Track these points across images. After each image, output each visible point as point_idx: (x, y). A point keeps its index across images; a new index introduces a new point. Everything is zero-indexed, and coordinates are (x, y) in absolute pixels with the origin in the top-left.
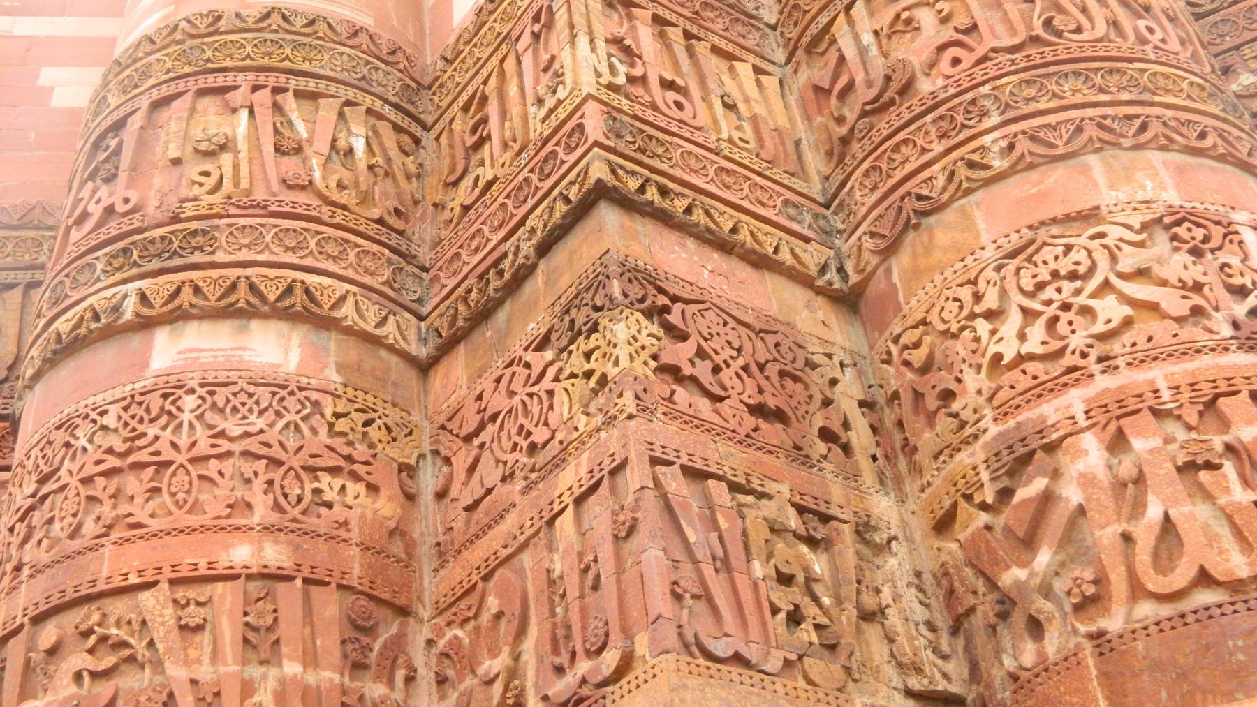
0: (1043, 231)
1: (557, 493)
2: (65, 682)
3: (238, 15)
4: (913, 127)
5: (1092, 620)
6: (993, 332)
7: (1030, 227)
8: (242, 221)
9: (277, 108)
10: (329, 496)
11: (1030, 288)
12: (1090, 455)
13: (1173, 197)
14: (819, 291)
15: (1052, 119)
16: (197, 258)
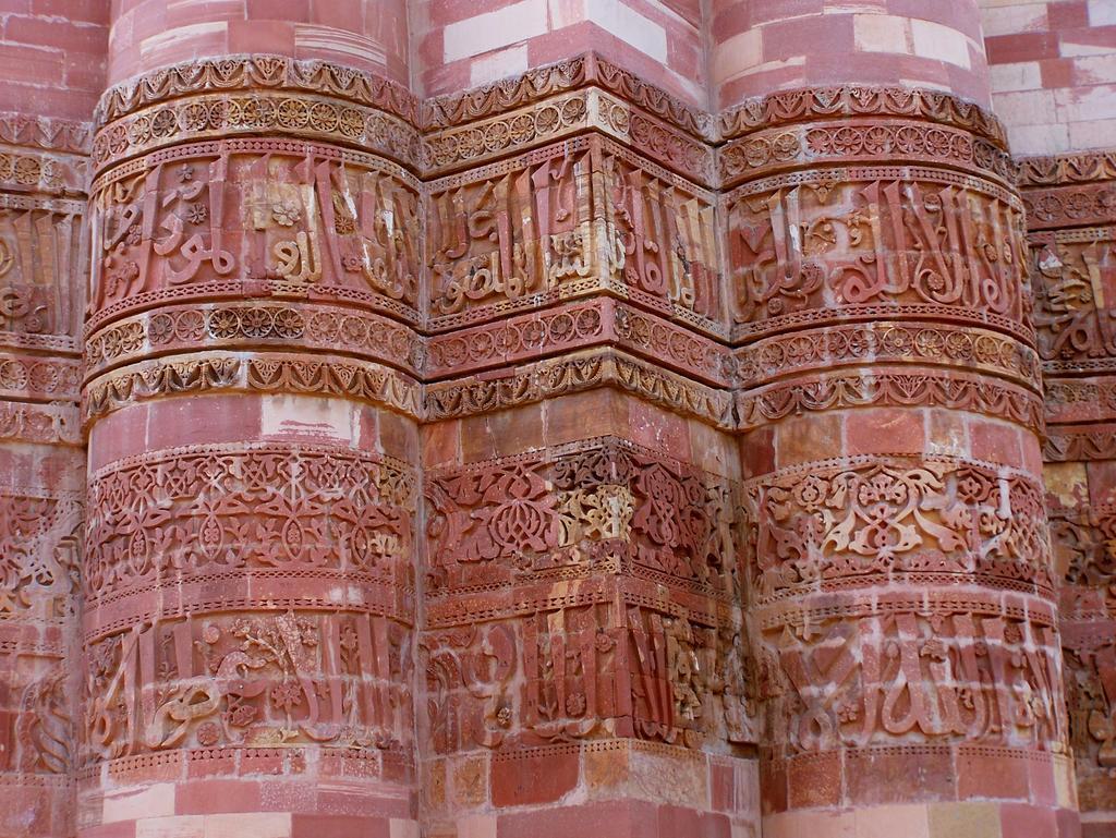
0: (882, 459)
1: (550, 597)
3: (295, 67)
4: (813, 331)
5: (850, 733)
6: (835, 524)
7: (875, 455)
8: (322, 309)
9: (335, 184)
10: (380, 549)
11: (865, 502)
12: (874, 635)
13: (966, 455)
14: (717, 429)
15: (909, 371)
16: (289, 339)
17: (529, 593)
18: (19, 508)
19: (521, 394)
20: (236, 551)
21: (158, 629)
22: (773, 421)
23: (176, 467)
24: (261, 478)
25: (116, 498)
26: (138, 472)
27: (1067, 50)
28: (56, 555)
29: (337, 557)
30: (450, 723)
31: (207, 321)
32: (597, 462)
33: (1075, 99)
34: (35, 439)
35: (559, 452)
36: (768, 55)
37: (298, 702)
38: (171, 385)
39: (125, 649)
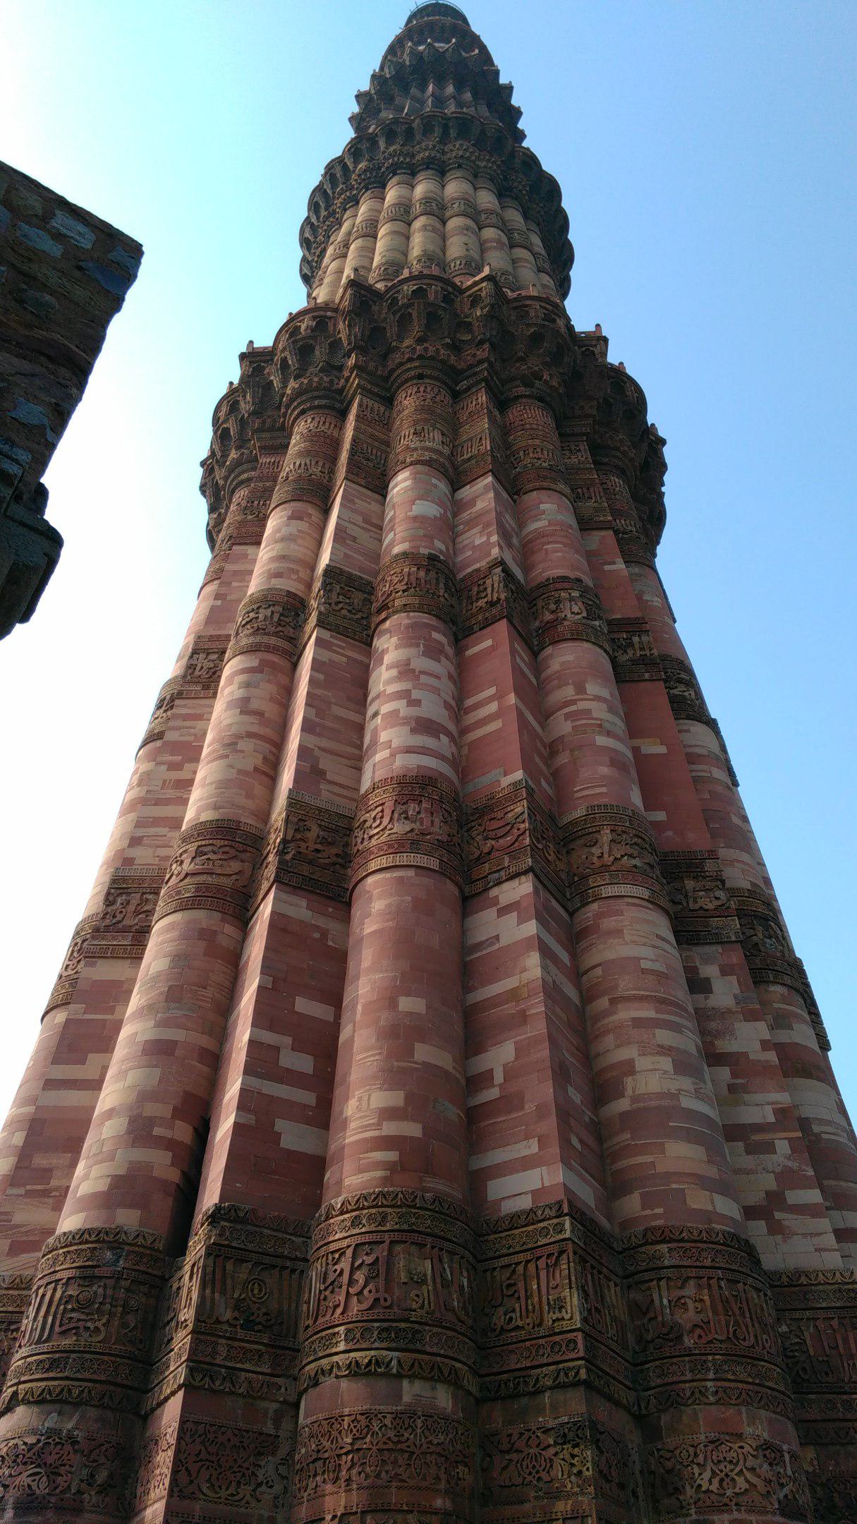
8: (435, 1330)
9: (441, 1260)
15: (732, 1385)
16: (418, 1346)
22: (660, 1411)
27: (778, 1215)
28: (277, 1469)
33: (785, 1241)
35: (556, 1422)
36: (644, 1208)
38: (355, 1371)
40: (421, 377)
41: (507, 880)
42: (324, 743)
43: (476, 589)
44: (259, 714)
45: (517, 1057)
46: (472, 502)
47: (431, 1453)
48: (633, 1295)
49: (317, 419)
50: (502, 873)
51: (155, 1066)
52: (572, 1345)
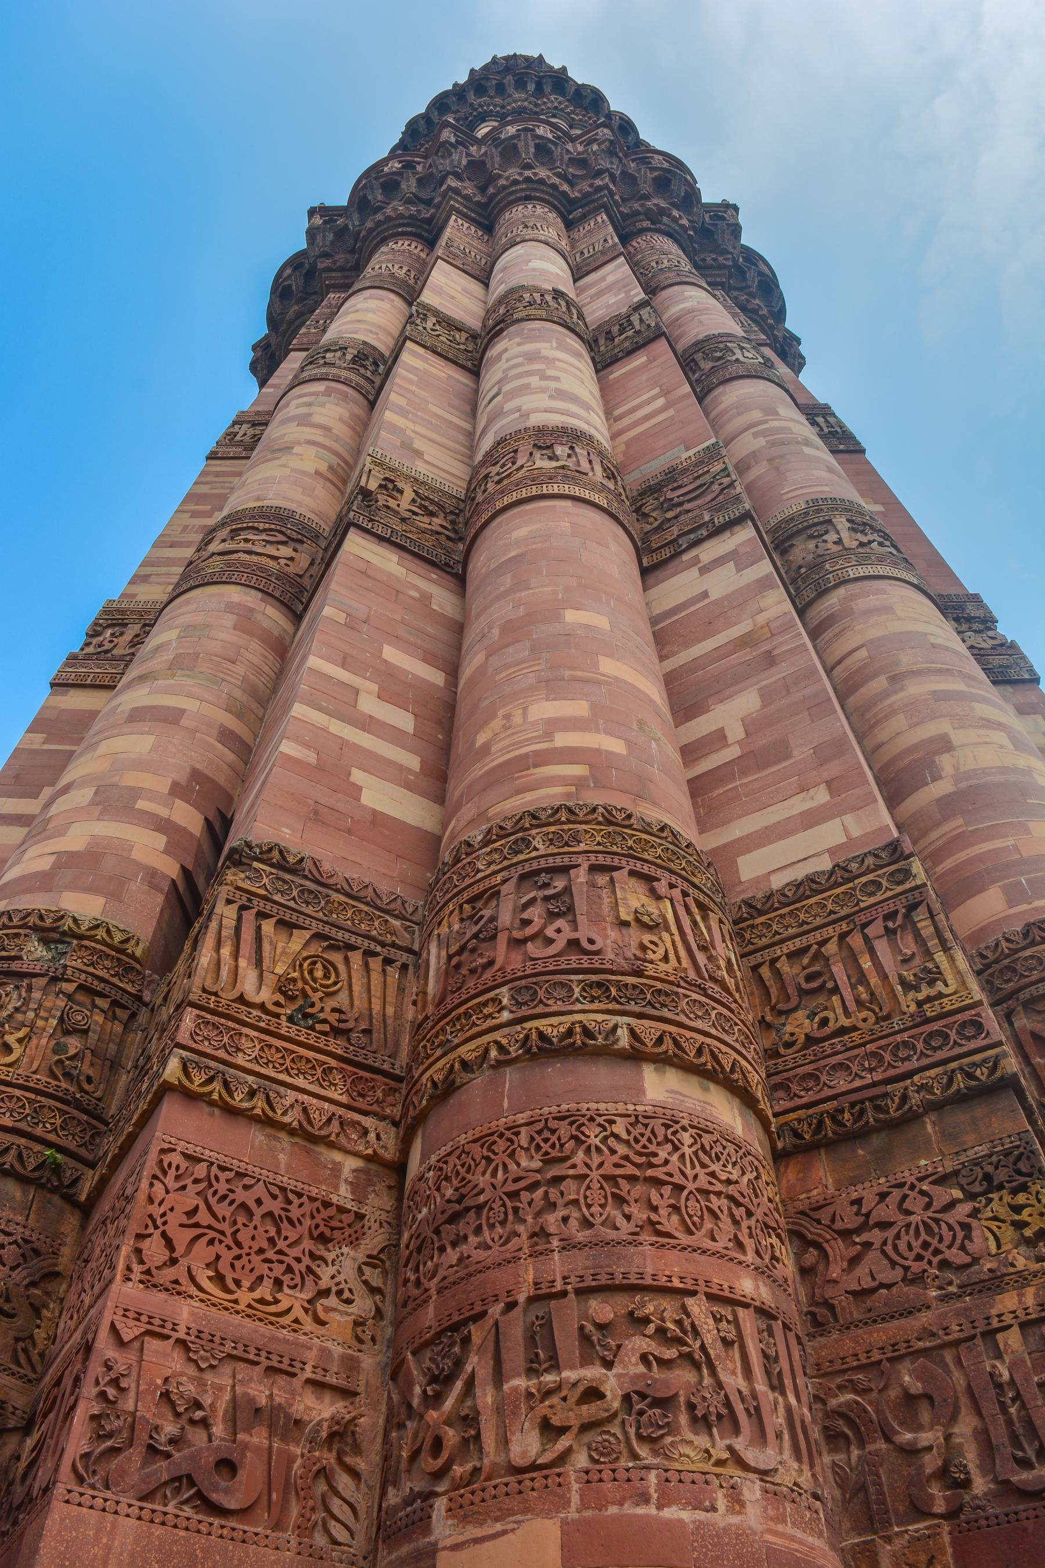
1: (994, 1312)
2: (633, 1360)
8: (695, 996)
10: (778, 1254)
16: (665, 1013)
17: (958, 1314)
18: (325, 1213)
19: (898, 1109)
20: (628, 1217)
21: (525, 1311)
23: (546, 1126)
24: (649, 1140)
25: (462, 1171)
26: (495, 1137)
29: (740, 1246)
30: (871, 1489)
31: (577, 990)
32: (1019, 1158)
34: (349, 1146)
35: (963, 1158)
36: (1011, 904)
37: (724, 1411)
39: (476, 1339)
40: (528, 198)
41: (711, 536)
42: (418, 428)
43: (615, 329)
44: (327, 429)
45: (764, 705)
46: (603, 279)
47: (718, 1194)
48: (1023, 1022)
49: (400, 243)
50: (704, 532)
51: (147, 733)
52: (969, 1032)
